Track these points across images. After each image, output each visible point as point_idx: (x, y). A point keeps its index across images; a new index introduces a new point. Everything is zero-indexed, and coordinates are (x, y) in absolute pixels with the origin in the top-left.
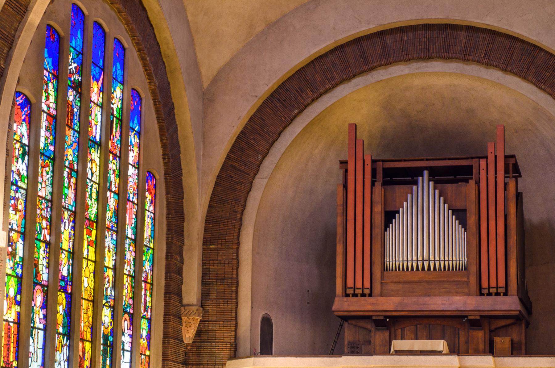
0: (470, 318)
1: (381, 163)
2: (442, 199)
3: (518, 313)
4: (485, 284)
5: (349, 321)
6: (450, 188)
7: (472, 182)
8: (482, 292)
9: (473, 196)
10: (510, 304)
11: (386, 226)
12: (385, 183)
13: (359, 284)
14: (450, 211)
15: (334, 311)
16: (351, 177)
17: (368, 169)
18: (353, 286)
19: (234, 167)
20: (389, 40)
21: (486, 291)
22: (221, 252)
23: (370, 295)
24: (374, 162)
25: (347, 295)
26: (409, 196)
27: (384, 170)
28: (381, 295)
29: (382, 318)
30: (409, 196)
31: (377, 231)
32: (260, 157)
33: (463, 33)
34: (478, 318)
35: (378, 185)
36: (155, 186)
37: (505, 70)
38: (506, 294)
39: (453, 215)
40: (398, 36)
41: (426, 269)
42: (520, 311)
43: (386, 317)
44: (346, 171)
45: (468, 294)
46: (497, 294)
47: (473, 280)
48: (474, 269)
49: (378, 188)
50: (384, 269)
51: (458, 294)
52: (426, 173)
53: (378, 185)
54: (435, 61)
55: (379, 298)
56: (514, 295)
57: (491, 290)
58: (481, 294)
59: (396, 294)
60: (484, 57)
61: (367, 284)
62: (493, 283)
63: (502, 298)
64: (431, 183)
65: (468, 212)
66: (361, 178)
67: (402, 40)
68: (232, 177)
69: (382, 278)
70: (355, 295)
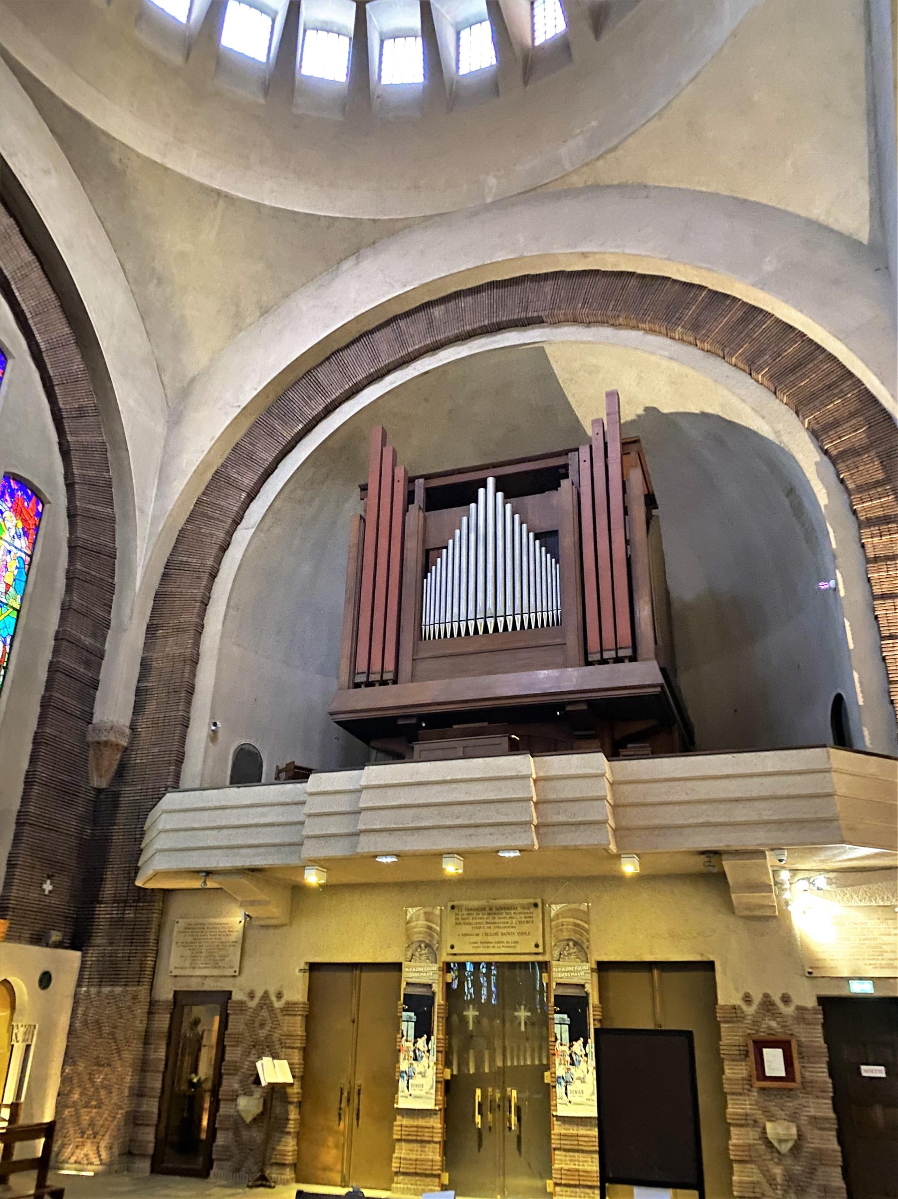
0: (568, 708)
1: (422, 480)
2: (517, 516)
3: (659, 689)
7: (565, 483)
10: (643, 674)
11: (426, 570)
14: (531, 535)
17: (400, 488)
18: (366, 670)
20: (437, 312)
21: (597, 657)
22: (171, 640)
23: (395, 682)
28: (413, 679)
29: (414, 721)
31: (410, 576)
32: (244, 495)
34: (584, 707)
36: (39, 515)
38: (633, 659)
39: (536, 538)
40: (451, 305)
41: (491, 630)
42: (661, 686)
45: (565, 665)
46: (618, 660)
47: (572, 639)
49: (415, 513)
50: (420, 635)
55: (410, 685)
57: (606, 655)
58: (588, 663)
61: (390, 666)
64: (500, 495)
69: (415, 651)
70: (370, 684)
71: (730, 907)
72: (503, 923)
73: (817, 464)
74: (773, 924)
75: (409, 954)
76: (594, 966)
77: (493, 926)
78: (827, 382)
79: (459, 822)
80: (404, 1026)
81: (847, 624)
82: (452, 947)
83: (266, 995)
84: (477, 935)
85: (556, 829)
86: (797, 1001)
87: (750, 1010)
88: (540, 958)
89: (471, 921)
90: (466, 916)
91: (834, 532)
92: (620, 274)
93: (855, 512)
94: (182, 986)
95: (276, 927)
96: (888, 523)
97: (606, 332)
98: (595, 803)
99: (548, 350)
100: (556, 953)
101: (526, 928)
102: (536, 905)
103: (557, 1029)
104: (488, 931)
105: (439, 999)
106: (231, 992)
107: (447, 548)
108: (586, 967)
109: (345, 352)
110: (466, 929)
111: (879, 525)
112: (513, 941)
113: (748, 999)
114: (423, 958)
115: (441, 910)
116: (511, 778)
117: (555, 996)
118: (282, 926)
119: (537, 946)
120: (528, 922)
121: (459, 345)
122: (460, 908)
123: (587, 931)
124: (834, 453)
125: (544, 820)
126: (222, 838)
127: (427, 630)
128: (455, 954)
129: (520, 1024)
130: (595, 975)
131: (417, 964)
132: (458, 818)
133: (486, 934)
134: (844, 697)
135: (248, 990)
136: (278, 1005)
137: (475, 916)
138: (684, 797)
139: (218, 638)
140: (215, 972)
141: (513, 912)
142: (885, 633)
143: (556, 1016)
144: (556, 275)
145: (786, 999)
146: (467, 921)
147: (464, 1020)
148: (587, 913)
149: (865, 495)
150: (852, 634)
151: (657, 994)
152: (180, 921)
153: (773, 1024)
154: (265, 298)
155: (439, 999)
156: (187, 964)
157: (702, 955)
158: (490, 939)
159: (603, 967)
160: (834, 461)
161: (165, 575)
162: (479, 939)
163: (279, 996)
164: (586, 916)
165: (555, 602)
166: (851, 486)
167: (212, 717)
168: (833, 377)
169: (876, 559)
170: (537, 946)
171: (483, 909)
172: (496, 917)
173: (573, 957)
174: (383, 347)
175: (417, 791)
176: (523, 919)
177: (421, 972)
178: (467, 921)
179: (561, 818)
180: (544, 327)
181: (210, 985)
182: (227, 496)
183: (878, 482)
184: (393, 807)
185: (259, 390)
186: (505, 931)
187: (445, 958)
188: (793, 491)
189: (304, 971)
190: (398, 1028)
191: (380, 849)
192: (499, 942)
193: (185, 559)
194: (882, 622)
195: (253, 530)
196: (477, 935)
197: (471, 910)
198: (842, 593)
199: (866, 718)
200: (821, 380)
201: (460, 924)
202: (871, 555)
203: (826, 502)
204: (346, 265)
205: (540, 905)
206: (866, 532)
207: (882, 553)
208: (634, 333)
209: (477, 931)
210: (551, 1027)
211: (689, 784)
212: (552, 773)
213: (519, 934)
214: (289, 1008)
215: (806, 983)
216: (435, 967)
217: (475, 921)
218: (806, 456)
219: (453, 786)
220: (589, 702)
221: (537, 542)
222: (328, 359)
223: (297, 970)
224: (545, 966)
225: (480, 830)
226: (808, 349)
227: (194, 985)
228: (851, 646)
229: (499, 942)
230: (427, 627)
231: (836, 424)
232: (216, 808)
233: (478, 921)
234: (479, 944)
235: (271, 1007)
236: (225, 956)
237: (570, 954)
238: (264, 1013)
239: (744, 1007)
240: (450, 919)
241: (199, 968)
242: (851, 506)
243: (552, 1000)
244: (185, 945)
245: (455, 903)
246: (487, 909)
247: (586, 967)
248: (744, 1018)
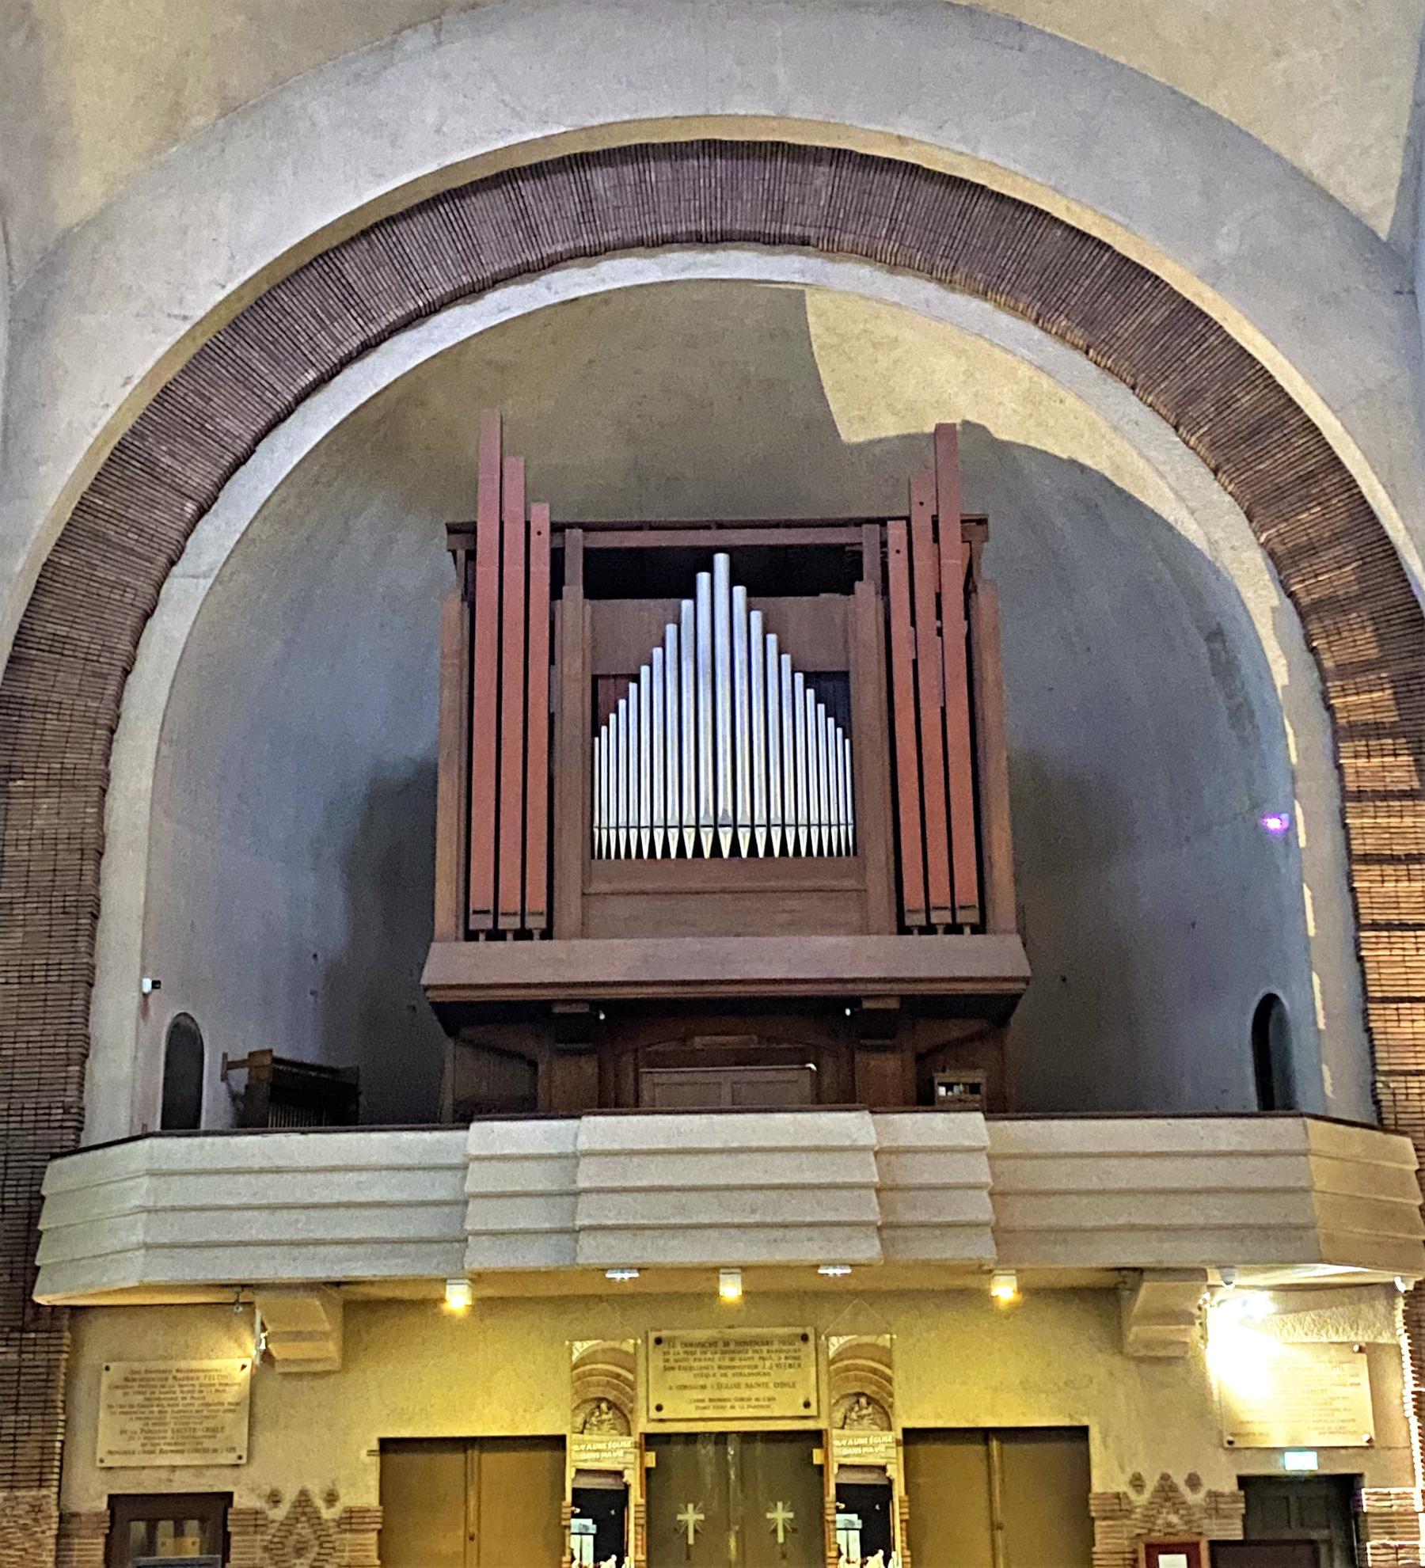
0: (867, 1005)
2: (772, 638)
4: (913, 897)
5: (467, 1032)
6: (794, 606)
8: (908, 922)
9: (869, 629)
12: (593, 591)
13: (510, 900)
14: (799, 677)
15: (427, 988)
16: (486, 571)
19: (98, 536)
20: (600, 179)
21: (920, 919)
22: (44, 803)
23: (547, 934)
24: (557, 528)
25: (471, 936)
26: (671, 629)
27: (589, 554)
30: (671, 629)
32: (190, 508)
33: (824, 169)
34: (893, 1004)
35: (574, 589)
37: (946, 281)
38: (979, 929)
40: (629, 172)
43: (597, 1005)
44: (471, 555)
45: (864, 930)
46: (954, 929)
48: (878, 852)
50: (592, 852)
51: (829, 927)
52: (721, 561)
53: (574, 589)
54: (737, 248)
56: (1005, 932)
58: (903, 930)
59: (627, 930)
60: (888, 237)
62: (940, 897)
63: (967, 940)
64: (740, 591)
65: (852, 678)
66: (514, 569)
67: (642, 181)
68: (94, 567)
69: (587, 877)
70: (496, 935)
71: (1116, 1341)
72: (749, 1367)
73: (1274, 610)
74: (1180, 1369)
75: (580, 1420)
76: (900, 1436)
77: (730, 1372)
78: (1302, 469)
79: (752, 1219)
80: (574, 1542)
81: (1307, 893)
82: (659, 1408)
83: (304, 1499)
84: (703, 1387)
85: (910, 1233)
86: (1208, 1485)
87: (1141, 1499)
88: (810, 1425)
90: (682, 1356)
91: (1296, 735)
92: (960, 183)
93: (1329, 708)
94: (126, 1485)
95: (316, 1375)
96: (1379, 737)
97: (928, 290)
98: (970, 1192)
99: (812, 300)
100: (838, 1416)
101: (787, 1375)
102: (805, 1338)
103: (841, 1537)
104: (723, 1380)
105: (636, 1497)
106: (230, 1495)
107: (636, 679)
108: (889, 1437)
109: (402, 227)
110: (685, 1378)
111: (1367, 737)
112: (766, 1396)
113: (1137, 1482)
114: (606, 1427)
115: (635, 1345)
116: (842, 1149)
117: (838, 1486)
118: (328, 1373)
119: (807, 1405)
120: (790, 1366)
121: (639, 256)
122: (672, 1341)
123: (889, 1380)
124: (1305, 600)
125: (890, 1219)
126: (281, 1227)
127: (605, 837)
128: (661, 1420)
129: (775, 1531)
130: (901, 1449)
131: (595, 1437)
132: (753, 1211)
133: (720, 1386)
134: (1284, 1000)
135: (267, 1489)
136: (327, 1514)
137: (698, 1355)
138: (1095, 1184)
139: (144, 806)
140: (197, 1460)
141: (765, 1348)
142: (1366, 919)
143: (840, 1517)
144: (838, 156)
145: (1193, 1482)
146: (683, 1364)
147: (681, 1530)
148: (888, 1352)
149: (1350, 684)
150: (1316, 915)
151: (997, 1478)
152: (112, 1365)
153: (1174, 1519)
154: (234, 81)
155: (636, 1497)
156: (136, 1445)
157: (1071, 1416)
158: (726, 1394)
159: (912, 1437)
160: (1303, 615)
161: (13, 659)
162: (706, 1395)
163: (331, 1498)
164: (886, 1356)
165: (845, 813)
166: (1329, 664)
167: (144, 971)
168: (1310, 464)
169: (1359, 795)
170: (807, 1405)
171: (713, 1344)
172: (737, 1356)
173: (866, 1421)
174: (487, 234)
175: (679, 1163)
177: (604, 1452)
178: (683, 1364)
179: (922, 1217)
180: (807, 255)
181: (183, 1484)
182: (152, 503)
183: (1369, 662)
184: (639, 1190)
185: (231, 287)
186: (752, 1380)
187: (643, 1425)
188: (1221, 640)
189: (370, 1453)
190: (562, 1547)
191: (607, 1260)
192: (742, 1400)
193: (62, 630)
194: (1363, 900)
195: (210, 581)
196: (703, 1387)
197: (691, 1345)
198: (1302, 842)
199: (1329, 1048)
200: (1291, 466)
201: (673, 1368)
202: (1352, 787)
203: (1286, 682)
204: (413, 42)
205: (812, 1338)
206: (1346, 747)
207: (1368, 786)
208: (976, 305)
209: (701, 1382)
210: (829, 1534)
211: (1104, 1163)
212: (903, 1142)
213: (777, 1385)
214: (351, 1519)
215: (1223, 1457)
216: (628, 1442)
218: (1259, 597)
219: (743, 1157)
220: (903, 998)
221: (811, 693)
222: (365, 233)
223: (364, 1453)
224: (817, 1438)
225: (790, 1234)
226: (1274, 403)
227: (150, 1484)
228: (1312, 932)
229: (742, 1400)
230: (604, 832)
231: (1311, 550)
232: (262, 1171)
233: (703, 1364)
234: (707, 1403)
235: (315, 1519)
236: (214, 1430)
237: (861, 1417)
238: (303, 1529)
239: (1132, 1495)
240: (657, 1360)
241: (161, 1451)
242: (1325, 696)
243: (832, 1491)
244: (127, 1411)
245: (664, 1334)
246: (720, 1344)
247: (889, 1437)
248: (1131, 1512)
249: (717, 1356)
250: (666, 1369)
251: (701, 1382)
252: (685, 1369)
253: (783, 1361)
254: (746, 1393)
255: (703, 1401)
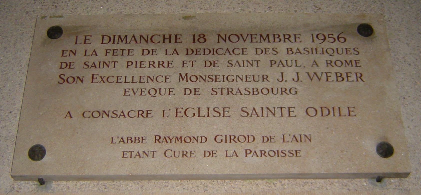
84: (143, 114)
89: (122, 70)
90: (101, 57)
120: (340, 77)
137: (137, 56)
141: (282, 47)
158: (194, 127)
172: (223, 59)
176: (322, 68)
178: (104, 72)
186: (257, 102)
192: (232, 139)
197: (123, 39)
209: (140, 103)
217: (136, 72)
229: (232, 139)
233: (147, 71)
234: (150, 145)
249: (177, 60)
250: (63, 80)
251: (140, 103)
252: (105, 80)
253: (322, 68)
254: (244, 126)
255: (140, 140)
